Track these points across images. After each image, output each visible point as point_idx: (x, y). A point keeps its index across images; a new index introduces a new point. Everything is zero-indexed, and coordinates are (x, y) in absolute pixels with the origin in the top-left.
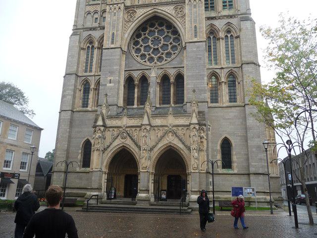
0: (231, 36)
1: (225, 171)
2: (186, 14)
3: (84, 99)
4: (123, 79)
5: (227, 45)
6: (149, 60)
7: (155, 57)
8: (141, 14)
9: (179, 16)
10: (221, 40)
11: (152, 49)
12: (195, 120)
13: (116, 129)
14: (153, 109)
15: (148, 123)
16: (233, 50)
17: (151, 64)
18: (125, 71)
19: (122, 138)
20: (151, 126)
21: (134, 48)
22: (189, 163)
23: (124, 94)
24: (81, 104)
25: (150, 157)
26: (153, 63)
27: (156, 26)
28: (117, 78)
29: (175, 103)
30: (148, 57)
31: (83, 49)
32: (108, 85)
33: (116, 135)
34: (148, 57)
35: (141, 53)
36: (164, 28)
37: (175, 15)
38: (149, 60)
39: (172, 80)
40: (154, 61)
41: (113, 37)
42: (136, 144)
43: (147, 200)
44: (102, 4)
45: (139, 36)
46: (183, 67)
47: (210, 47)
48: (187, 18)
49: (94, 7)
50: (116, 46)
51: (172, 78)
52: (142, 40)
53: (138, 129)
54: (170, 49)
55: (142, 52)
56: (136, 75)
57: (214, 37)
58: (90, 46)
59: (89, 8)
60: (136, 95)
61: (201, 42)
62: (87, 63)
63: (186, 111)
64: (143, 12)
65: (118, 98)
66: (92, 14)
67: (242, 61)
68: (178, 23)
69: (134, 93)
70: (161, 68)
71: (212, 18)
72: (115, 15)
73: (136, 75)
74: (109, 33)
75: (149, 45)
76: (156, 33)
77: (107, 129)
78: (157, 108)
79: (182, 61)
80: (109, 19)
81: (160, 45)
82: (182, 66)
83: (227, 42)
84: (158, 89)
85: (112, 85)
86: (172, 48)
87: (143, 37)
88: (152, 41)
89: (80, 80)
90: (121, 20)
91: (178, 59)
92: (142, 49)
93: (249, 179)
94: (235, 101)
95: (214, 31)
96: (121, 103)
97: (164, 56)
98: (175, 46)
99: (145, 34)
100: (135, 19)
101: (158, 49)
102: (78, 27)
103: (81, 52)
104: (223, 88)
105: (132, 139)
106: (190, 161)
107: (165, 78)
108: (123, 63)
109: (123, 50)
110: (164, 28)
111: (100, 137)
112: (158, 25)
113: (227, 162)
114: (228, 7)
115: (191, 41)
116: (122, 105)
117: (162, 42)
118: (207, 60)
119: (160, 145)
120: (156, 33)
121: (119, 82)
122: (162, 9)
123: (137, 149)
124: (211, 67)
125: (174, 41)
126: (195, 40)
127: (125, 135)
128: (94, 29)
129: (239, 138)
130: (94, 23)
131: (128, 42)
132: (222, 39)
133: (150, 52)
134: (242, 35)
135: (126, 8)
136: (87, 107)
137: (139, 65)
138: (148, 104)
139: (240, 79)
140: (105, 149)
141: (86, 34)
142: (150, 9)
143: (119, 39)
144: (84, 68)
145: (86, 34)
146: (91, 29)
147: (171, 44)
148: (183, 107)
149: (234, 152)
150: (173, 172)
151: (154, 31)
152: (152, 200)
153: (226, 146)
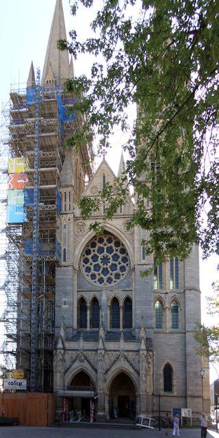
1: (167, 394)
5: (172, 267)
7: (105, 278)
11: (101, 269)
12: (143, 346)
13: (74, 352)
15: (102, 347)
19: (81, 362)
20: (106, 351)
22: (138, 386)
25: (105, 379)
29: (124, 327)
33: (74, 358)
34: (98, 277)
39: (121, 304)
42: (92, 367)
43: (104, 417)
45: (88, 252)
53: (94, 353)
55: (92, 271)
56: (89, 297)
60: (88, 318)
63: (135, 337)
67: (185, 287)
73: (89, 297)
76: (105, 251)
77: (67, 352)
79: (129, 285)
84: (109, 312)
85: (67, 306)
87: (92, 254)
93: (186, 401)
94: (177, 328)
96: (75, 325)
98: (124, 267)
101: (107, 268)
105: (89, 363)
106: (139, 384)
107: (115, 300)
111: (61, 360)
113: (168, 386)
116: (76, 328)
119: (113, 369)
120: (105, 251)
121: (73, 304)
123: (94, 373)
125: (122, 261)
127: (82, 358)
129: (179, 363)
139: (182, 306)
140: (66, 371)
149: (174, 377)
150: (123, 393)
152: (108, 417)
153: (168, 370)
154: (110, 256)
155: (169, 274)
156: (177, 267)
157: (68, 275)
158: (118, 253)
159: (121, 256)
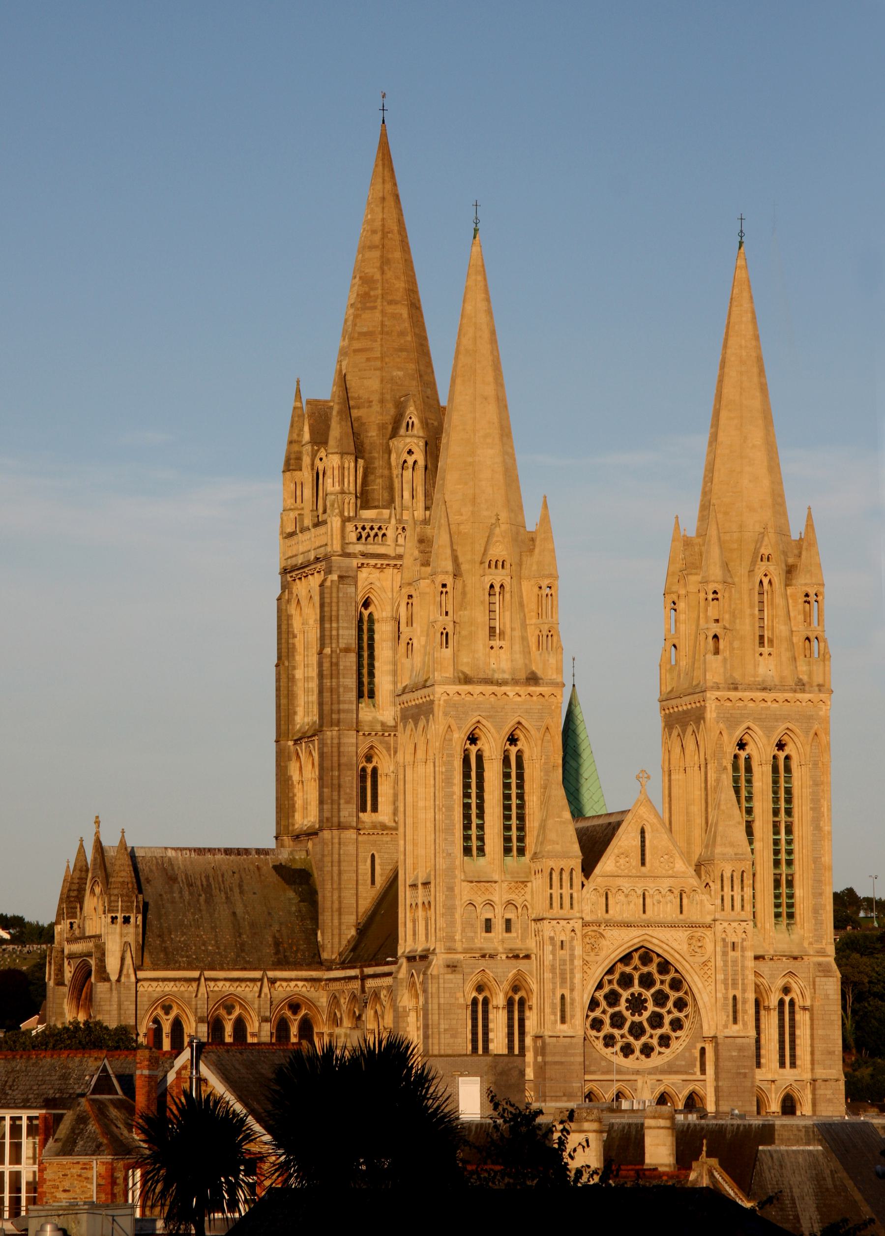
16: (793, 1035)
40: (632, 1052)
55: (607, 1029)
68: (696, 978)
80: (551, 957)
81: (646, 1014)
86: (672, 1023)
88: (627, 1001)
154: (648, 994)
156: (792, 1020)
157: (573, 1055)
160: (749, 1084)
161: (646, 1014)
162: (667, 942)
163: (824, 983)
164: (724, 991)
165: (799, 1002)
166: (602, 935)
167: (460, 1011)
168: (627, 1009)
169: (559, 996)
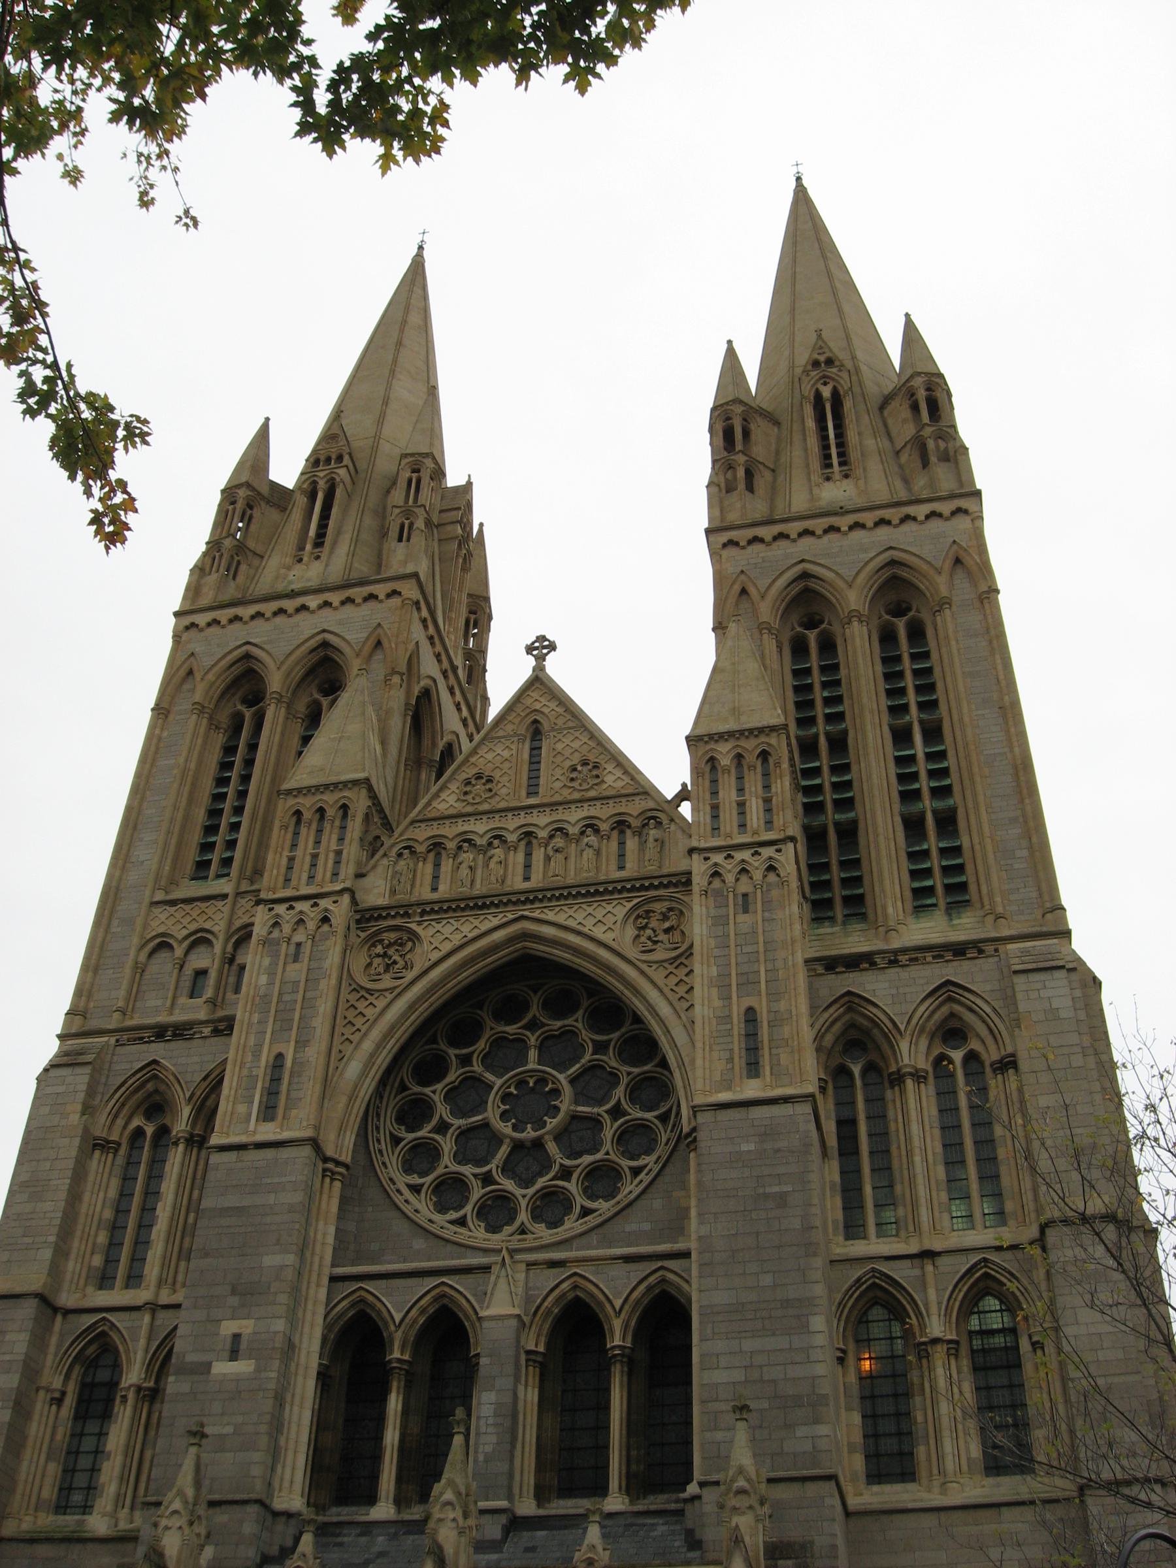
0: (972, 1057)
2: (697, 949)
3: (73, 1452)
4: (318, 1332)
5: (948, 1110)
6: (482, 1212)
8: (447, 947)
9: (660, 954)
10: (909, 1083)
11: (503, 1151)
14: (493, 1529)
17: (495, 1240)
18: (333, 1279)
21: (396, 1141)
23: (320, 1425)
24: (49, 1492)
26: (508, 1229)
27: (535, 1011)
28: (280, 1325)
29: (636, 1486)
30: (477, 1192)
31: (104, 1145)
32: (223, 1368)
34: (477, 1192)
35: (440, 1170)
36: (577, 1021)
37: (632, 953)
38: (482, 1212)
39: (618, 1337)
41: (276, 1080)
44: (238, 894)
45: (430, 1071)
46: (686, 1255)
47: (846, 1125)
48: (703, 970)
49: (195, 910)
50: (286, 1135)
51: (617, 1324)
52: (450, 1095)
54: (607, 1146)
55: (447, 1163)
57: (870, 1068)
58: (150, 1130)
59: (164, 921)
60: (391, 1436)
61: (786, 1100)
62: (116, 1228)
64: (457, 940)
65: (275, 1454)
66: (179, 952)
68: (653, 995)
69: (380, 1420)
70: (553, 1264)
71: (854, 962)
72: (296, 959)
74: (257, 1054)
75: (486, 1125)
76: (533, 1054)
78: (516, 1524)
79: (677, 1224)
80: (264, 979)
81: (552, 1123)
82: (680, 1246)
83: (946, 1095)
85: (243, 1367)
86: (622, 1138)
88: (506, 1097)
89: (60, 1333)
90: (327, 986)
91: (656, 1203)
92: (447, 1145)
95: (867, 1032)
97: (572, 1186)
98: (643, 1128)
99: (466, 1060)
100: (410, 975)
101: (538, 1144)
102: (94, 1023)
103: (94, 1163)
104: (942, 1382)
108: (326, 1233)
109: (330, 1152)
110: (577, 1021)
112: (546, 1005)
114: (941, 897)
115: (724, 1096)
117: (565, 1104)
118: (834, 1207)
120: (533, 1054)
121: (290, 1348)
122: (561, 918)
124: (859, 1248)
126: (752, 1089)
128: (180, 1032)
130: (183, 1000)
131: (359, 1108)
132: (919, 1077)
133: (492, 1166)
134: (1024, 1044)
135: (365, 917)
136: (86, 1509)
137: (419, 1244)
138: (449, 1495)
141: (136, 1056)
142: (496, 922)
143: (310, 1090)
144: (97, 1261)
145: (136, 1056)
146: (160, 1033)
147: (617, 1112)
148: (680, 1513)
151: (520, 1043)
155: (935, 1145)
158: (611, 1060)
159: (627, 1072)
160: (796, 1224)
161: (552, 1123)
162: (580, 928)
163: (1038, 986)
164: (717, 1003)
165: (991, 1054)
166: (414, 937)
167: (67, 1141)
168: (504, 1116)
169: (265, 1058)
